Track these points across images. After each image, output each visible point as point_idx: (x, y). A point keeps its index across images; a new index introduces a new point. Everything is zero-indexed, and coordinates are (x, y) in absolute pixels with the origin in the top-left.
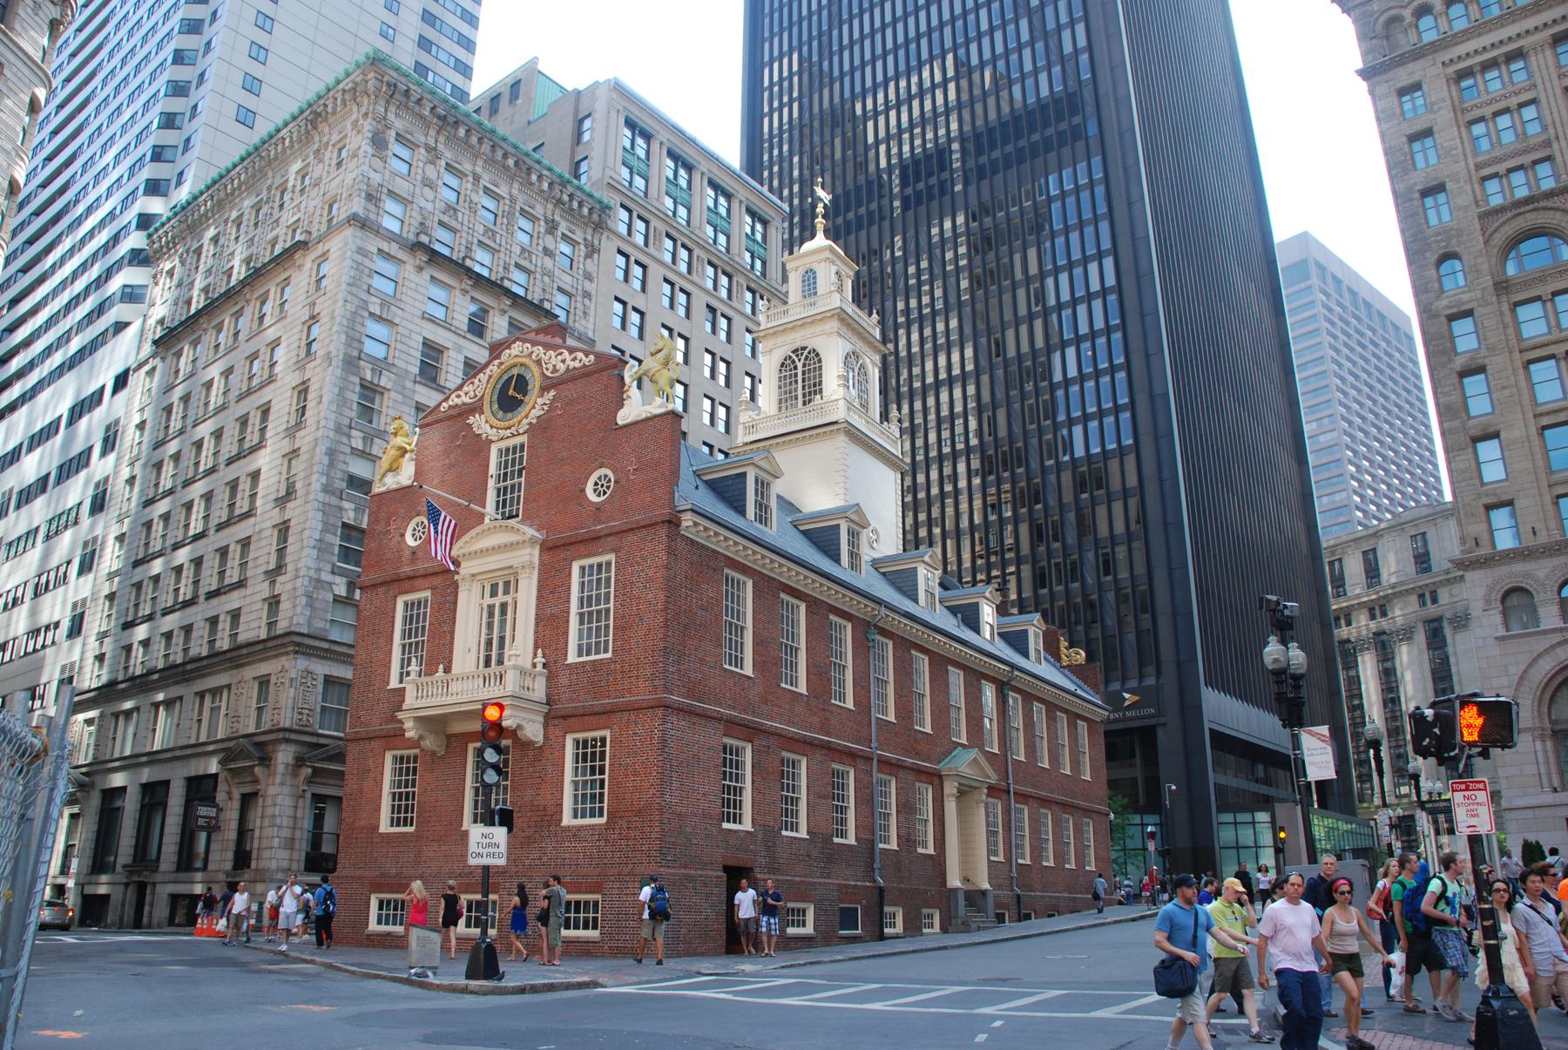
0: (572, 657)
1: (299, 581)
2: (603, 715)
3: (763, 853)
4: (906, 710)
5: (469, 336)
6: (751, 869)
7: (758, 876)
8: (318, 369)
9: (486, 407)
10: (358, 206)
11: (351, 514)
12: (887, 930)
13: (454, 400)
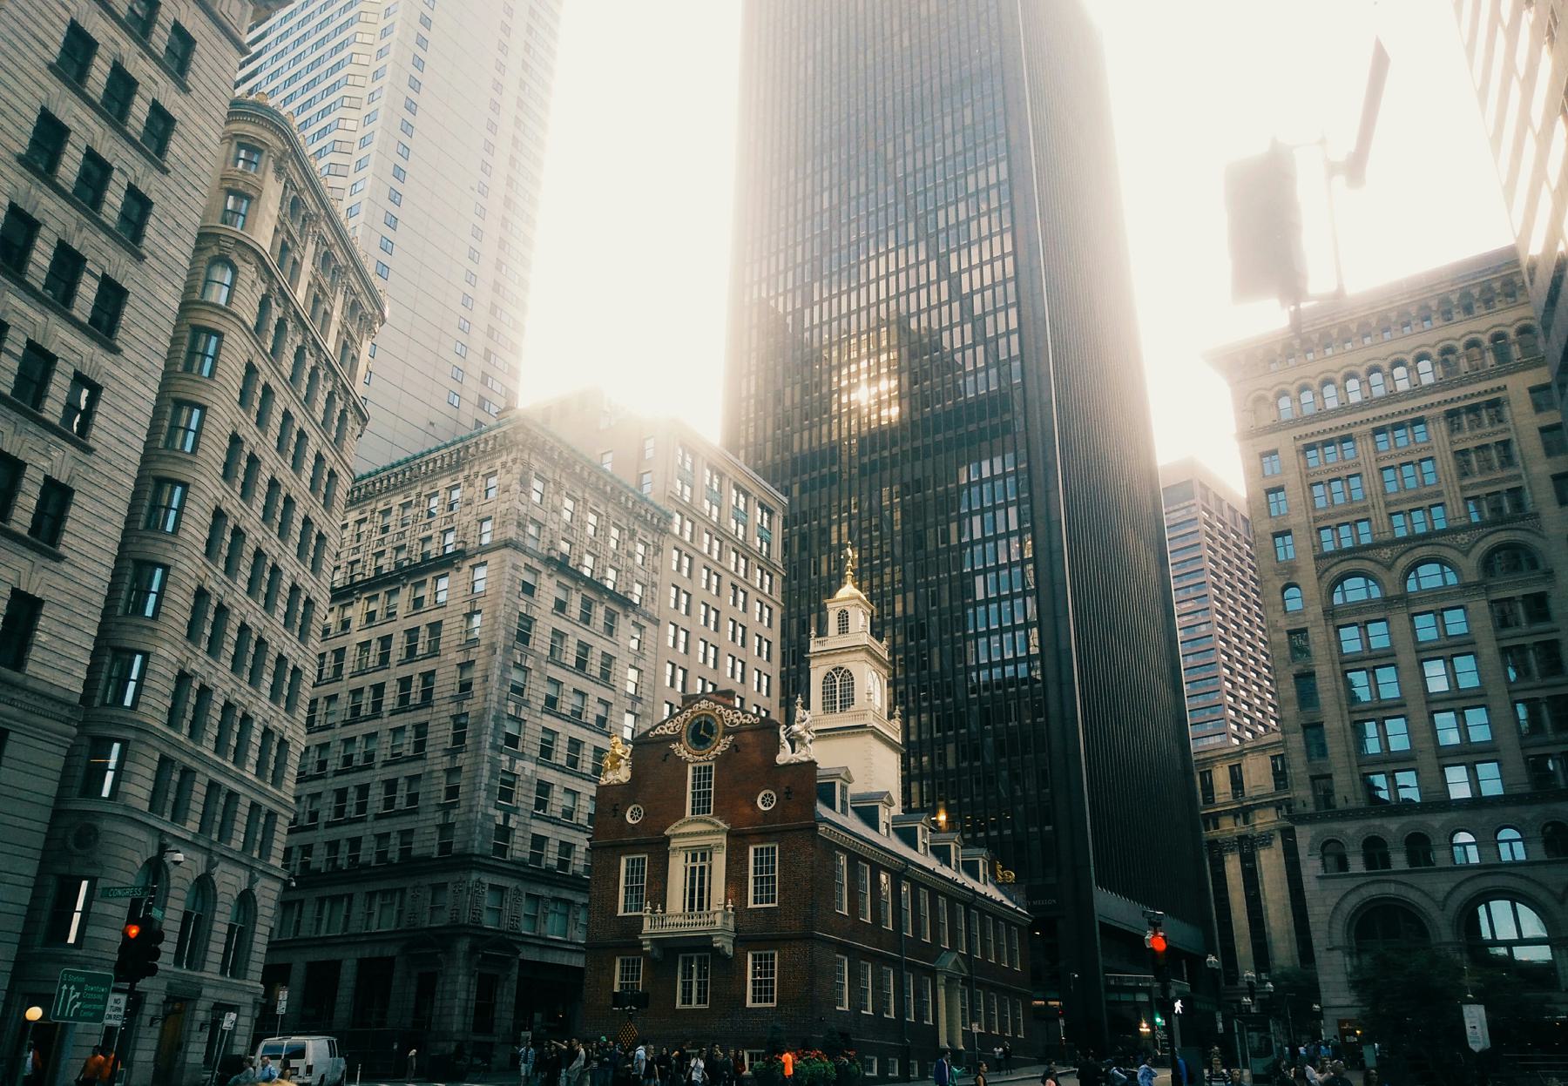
0: (751, 905)
1: (472, 816)
8: (483, 655)
9: (684, 739)
10: (512, 532)
13: (659, 731)
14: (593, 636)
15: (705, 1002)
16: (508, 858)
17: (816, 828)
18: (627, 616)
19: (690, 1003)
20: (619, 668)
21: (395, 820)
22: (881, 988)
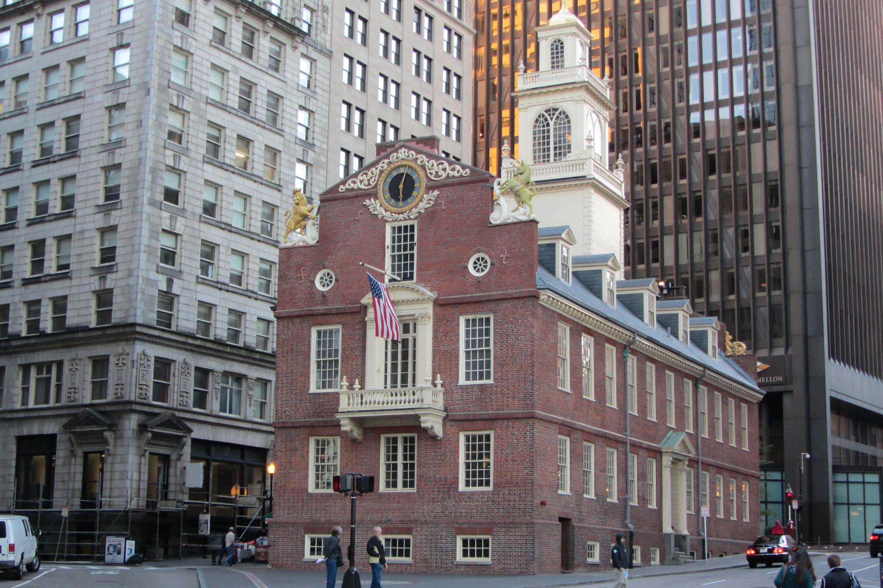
0: (462, 381)
1: (132, 281)
2: (491, 421)
3: (576, 510)
4: (643, 408)
5: (243, 58)
6: (570, 520)
7: (575, 524)
8: (133, 96)
11: (168, 222)
12: (634, 562)
13: (350, 185)
14: (259, 74)
15: (412, 485)
16: (173, 328)
17: (536, 297)
18: (295, 48)
19: (395, 485)
20: (288, 109)
21: (44, 286)
22: (604, 471)
